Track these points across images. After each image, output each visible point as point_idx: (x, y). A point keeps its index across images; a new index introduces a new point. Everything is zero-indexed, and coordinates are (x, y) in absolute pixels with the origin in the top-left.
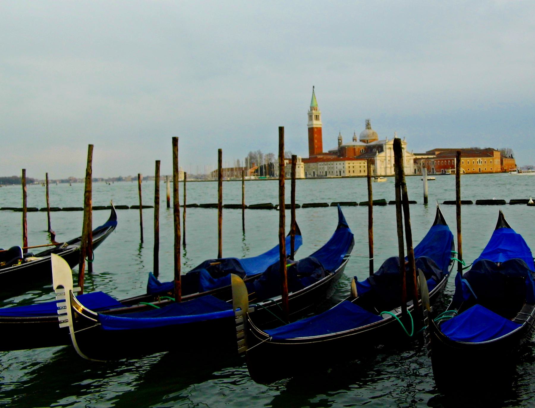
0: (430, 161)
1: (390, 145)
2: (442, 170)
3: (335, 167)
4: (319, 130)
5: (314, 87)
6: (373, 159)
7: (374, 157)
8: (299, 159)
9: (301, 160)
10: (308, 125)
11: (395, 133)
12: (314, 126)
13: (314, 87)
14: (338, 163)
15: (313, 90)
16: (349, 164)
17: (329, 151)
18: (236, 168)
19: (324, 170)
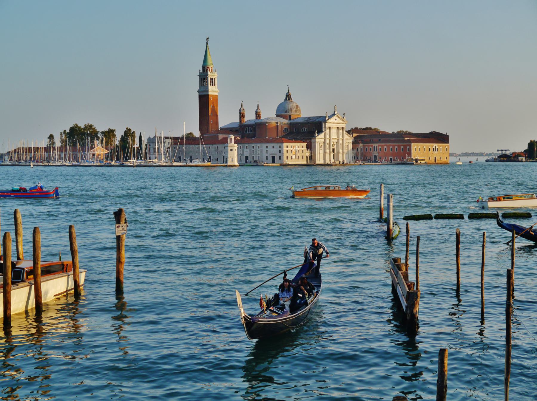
0: (372, 146)
1: (331, 123)
2: (391, 159)
3: (264, 152)
4: (216, 98)
5: (207, 39)
6: (308, 141)
7: (311, 139)
8: (231, 139)
9: (233, 141)
10: (198, 91)
11: (335, 108)
12: (210, 93)
13: (207, 39)
14: (270, 146)
15: (207, 43)
16: (287, 147)
17: (221, 128)
18: (45, 148)
19: (243, 155)
